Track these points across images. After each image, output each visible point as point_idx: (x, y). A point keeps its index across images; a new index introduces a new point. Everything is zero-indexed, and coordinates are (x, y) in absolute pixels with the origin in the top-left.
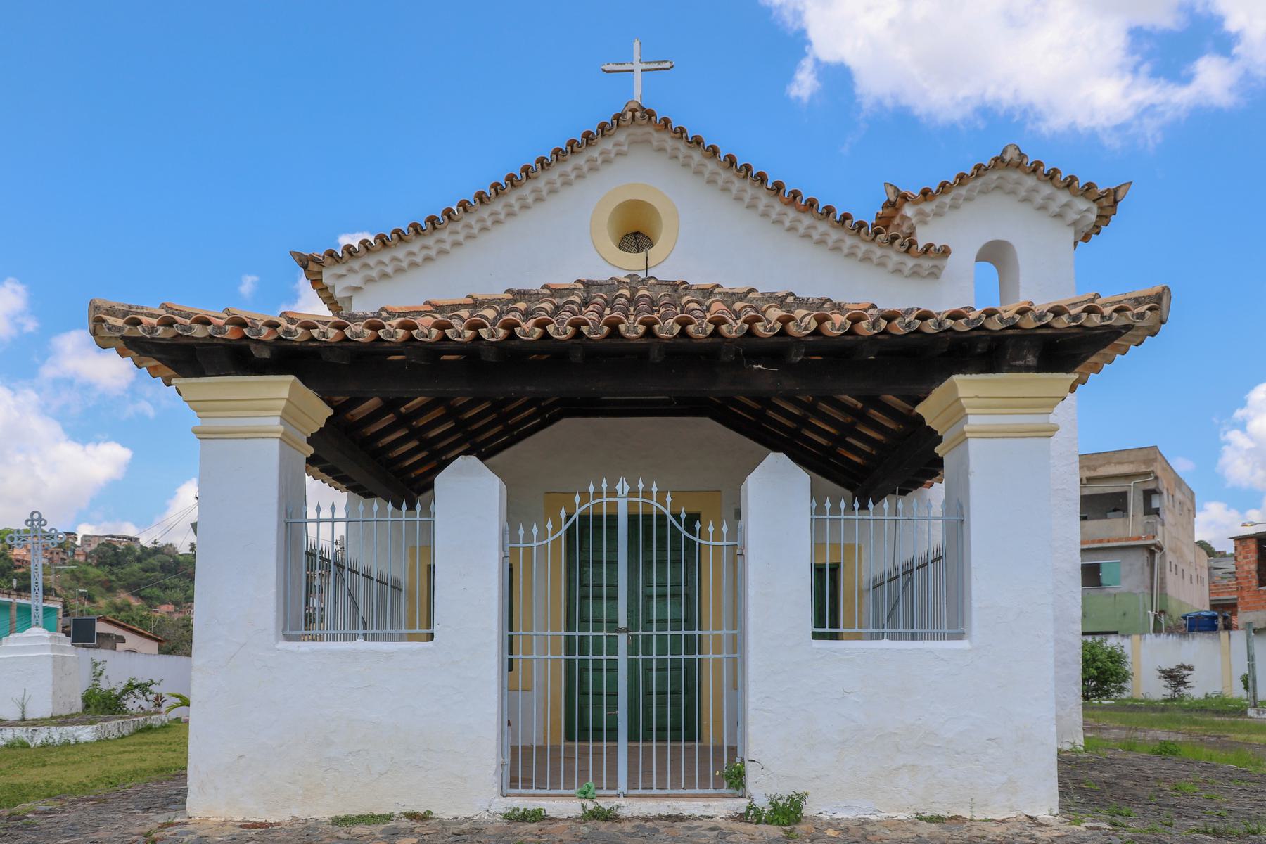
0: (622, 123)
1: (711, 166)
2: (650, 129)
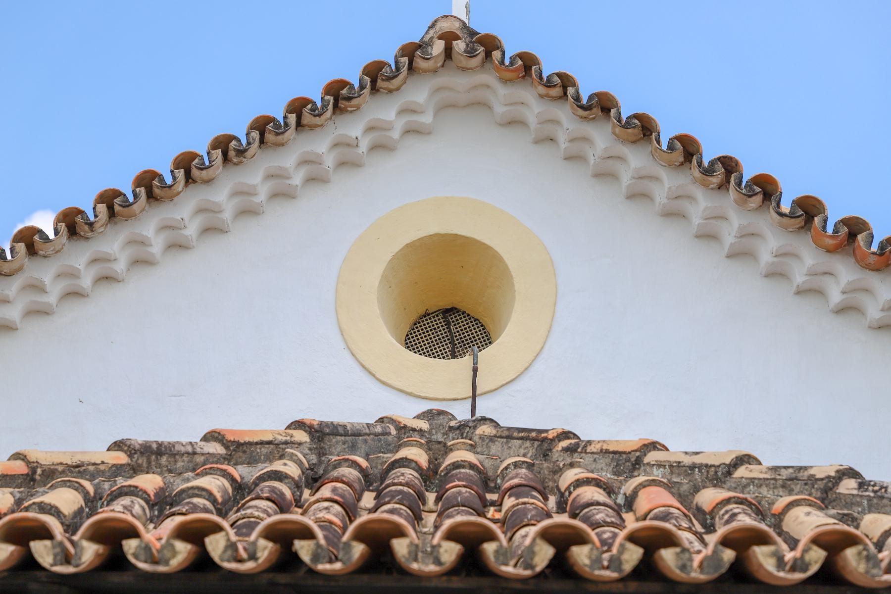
0: (420, 63)
2: (488, 78)
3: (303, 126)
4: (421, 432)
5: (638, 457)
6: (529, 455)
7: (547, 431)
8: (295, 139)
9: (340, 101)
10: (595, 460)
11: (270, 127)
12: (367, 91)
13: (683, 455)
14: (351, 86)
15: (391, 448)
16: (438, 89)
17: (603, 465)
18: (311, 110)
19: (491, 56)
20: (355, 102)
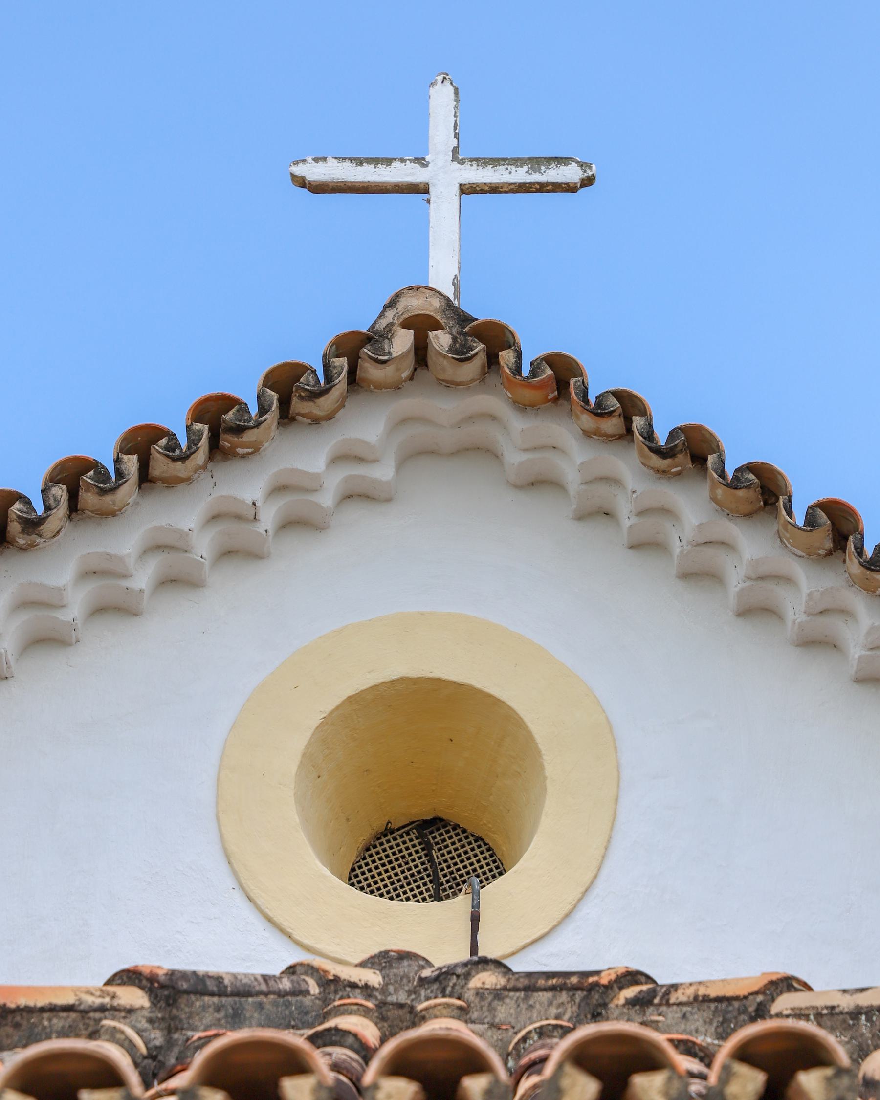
0: (371, 371)
1: (753, 546)
3: (153, 481)
4: (367, 989)
5: (760, 1004)
6: (567, 1017)
7: (598, 973)
8: (137, 503)
9: (223, 436)
10: (684, 1016)
11: (88, 478)
12: (272, 416)
13: (839, 995)
14: (243, 408)
15: (309, 1018)
16: (405, 421)
17: (699, 1024)
18: (168, 448)
19: (498, 363)
20: (249, 436)
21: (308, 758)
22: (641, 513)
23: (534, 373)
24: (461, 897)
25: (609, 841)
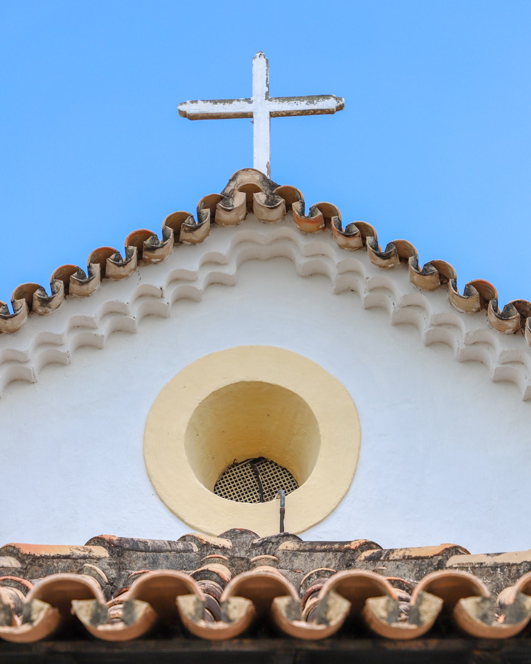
0: (222, 216)
1: (435, 307)
2: (289, 230)
4: (224, 549)
5: (440, 561)
6: (332, 566)
7: (349, 542)
12: (170, 241)
15: (193, 564)
16: (241, 242)
17: (406, 571)
19: (292, 209)
20: (158, 252)
21: (191, 425)
22: (372, 290)
23: (312, 214)
24: (274, 500)
25: (355, 471)
